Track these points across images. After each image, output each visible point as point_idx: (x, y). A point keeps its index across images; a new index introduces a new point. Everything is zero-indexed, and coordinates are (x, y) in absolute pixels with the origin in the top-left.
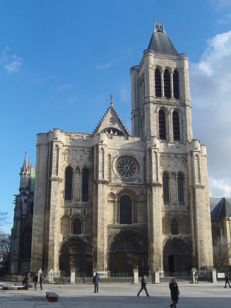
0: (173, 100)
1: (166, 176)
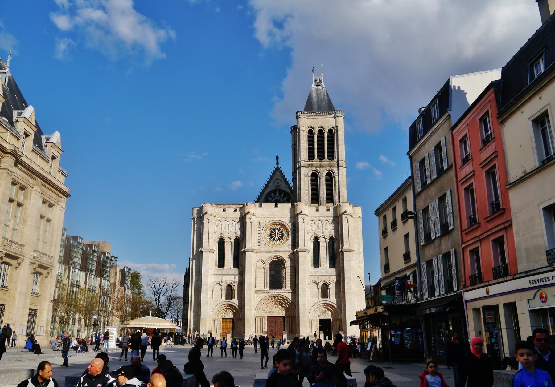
0: (326, 161)
1: (316, 241)
